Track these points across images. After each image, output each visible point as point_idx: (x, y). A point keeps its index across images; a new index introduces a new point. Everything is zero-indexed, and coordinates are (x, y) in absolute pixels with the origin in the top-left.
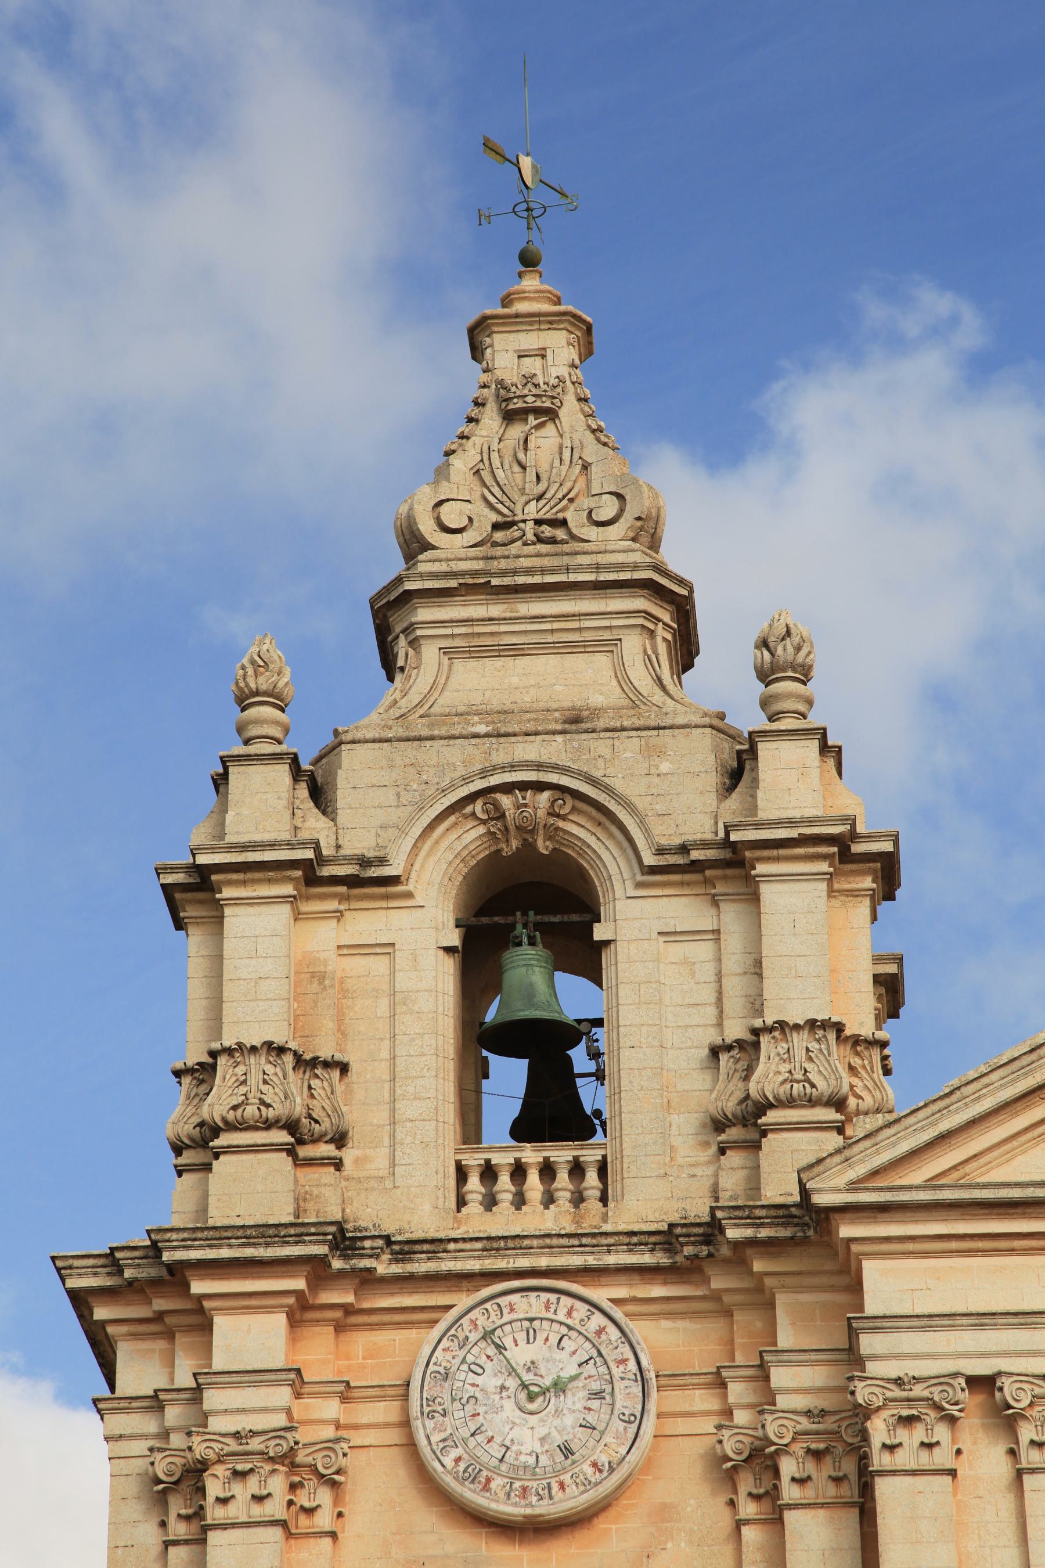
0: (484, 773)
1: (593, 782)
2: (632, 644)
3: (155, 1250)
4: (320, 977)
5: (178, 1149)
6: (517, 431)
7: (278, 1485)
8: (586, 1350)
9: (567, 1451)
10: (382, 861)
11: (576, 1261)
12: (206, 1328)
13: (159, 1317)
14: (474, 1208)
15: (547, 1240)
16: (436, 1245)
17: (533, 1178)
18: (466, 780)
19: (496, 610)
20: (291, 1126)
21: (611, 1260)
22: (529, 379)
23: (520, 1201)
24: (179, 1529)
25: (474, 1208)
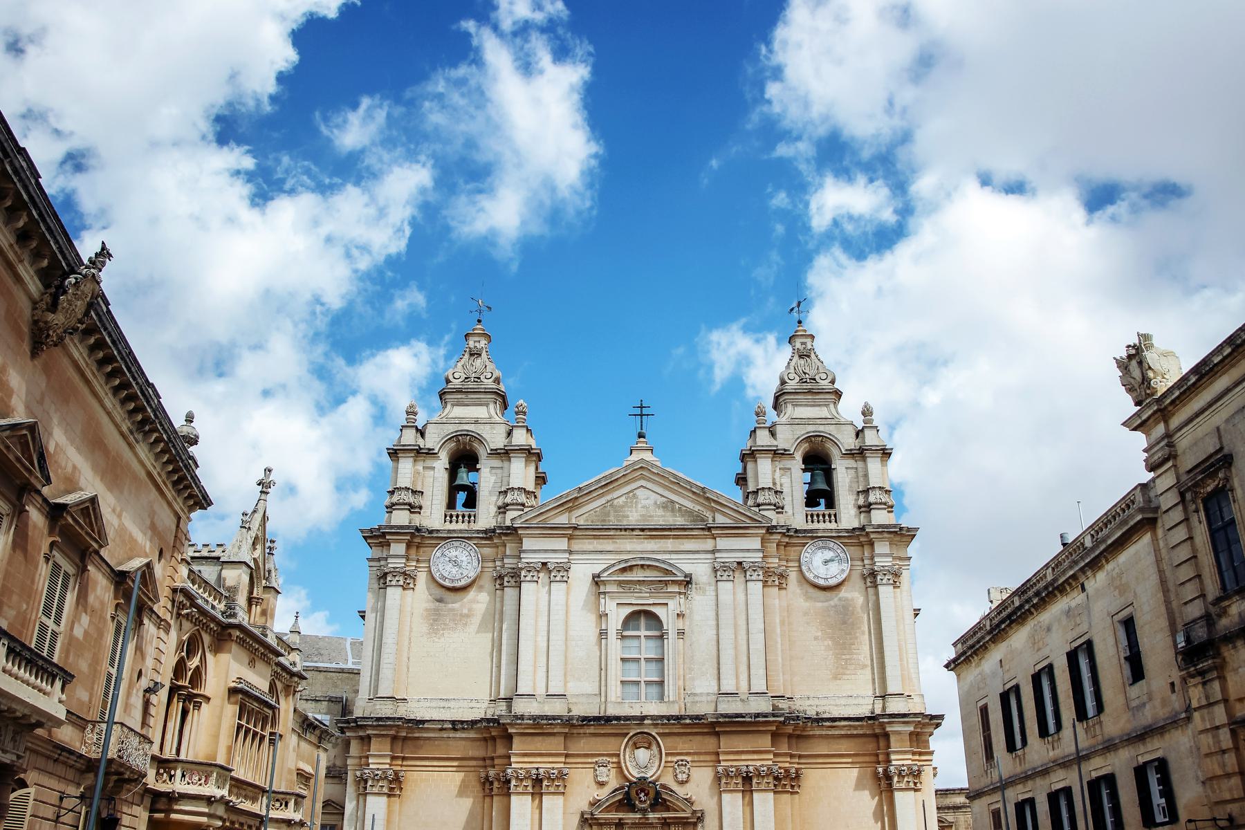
0: (456, 432)
1: (478, 434)
2: (492, 406)
3: (379, 529)
4: (419, 473)
5: (387, 507)
6: (472, 358)
7: (401, 579)
8: (467, 554)
10: (433, 449)
11: (467, 535)
12: (389, 545)
13: (381, 542)
14: (448, 523)
15: (461, 531)
16: (438, 531)
17: (460, 518)
18: (452, 433)
19: (463, 396)
20: (410, 504)
22: (475, 347)
24: (382, 586)
25: (448, 523)
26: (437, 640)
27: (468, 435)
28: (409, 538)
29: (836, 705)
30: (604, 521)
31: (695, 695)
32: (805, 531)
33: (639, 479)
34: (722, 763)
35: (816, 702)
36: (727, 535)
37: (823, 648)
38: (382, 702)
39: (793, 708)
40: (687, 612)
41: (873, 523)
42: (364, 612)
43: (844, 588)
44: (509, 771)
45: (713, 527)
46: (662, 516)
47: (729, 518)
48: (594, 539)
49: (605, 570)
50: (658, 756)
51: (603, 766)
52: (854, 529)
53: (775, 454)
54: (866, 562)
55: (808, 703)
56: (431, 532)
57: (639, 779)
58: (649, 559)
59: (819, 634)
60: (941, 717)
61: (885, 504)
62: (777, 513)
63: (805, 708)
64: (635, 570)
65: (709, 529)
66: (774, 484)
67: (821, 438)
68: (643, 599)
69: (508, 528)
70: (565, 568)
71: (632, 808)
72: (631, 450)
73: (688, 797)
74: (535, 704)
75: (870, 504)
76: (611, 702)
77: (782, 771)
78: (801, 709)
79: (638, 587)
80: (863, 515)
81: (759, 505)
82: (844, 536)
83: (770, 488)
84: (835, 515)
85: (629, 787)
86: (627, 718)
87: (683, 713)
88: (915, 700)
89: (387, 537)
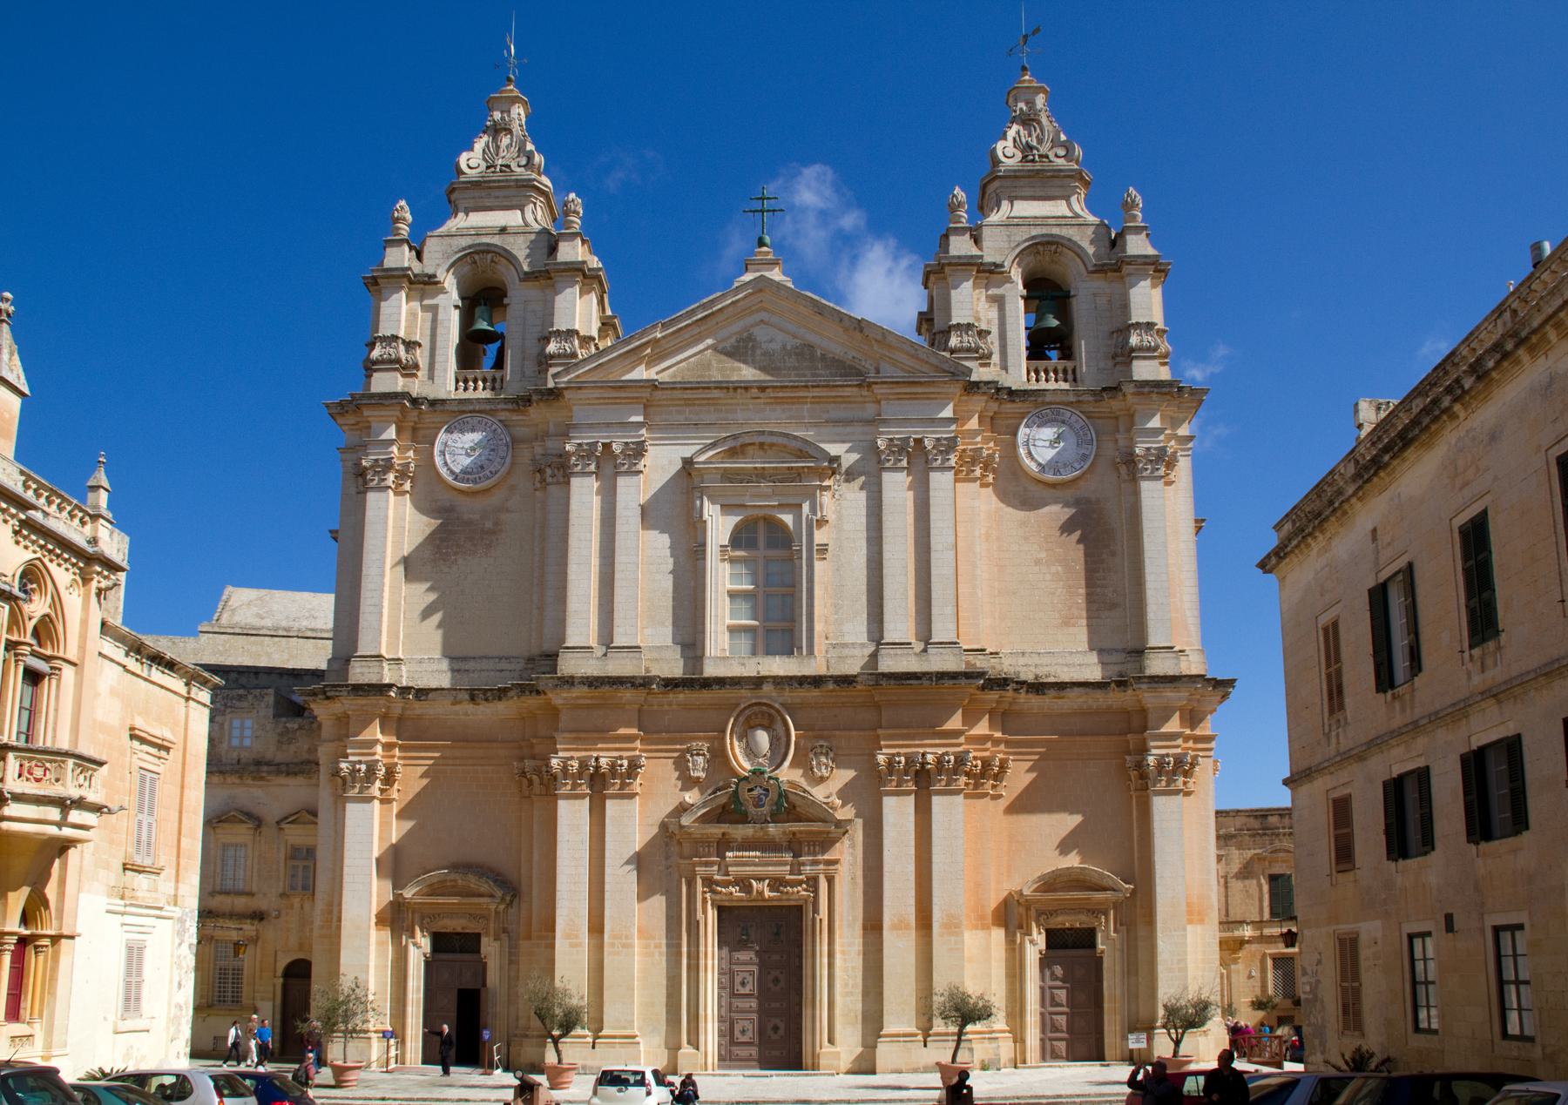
9: (482, 467)
21: (499, 407)
23: (475, 389)
26: (446, 570)
27: (488, 252)
28: (398, 414)
29: (1066, 665)
30: (702, 376)
31: (844, 645)
32: (1025, 392)
33: (758, 311)
34: (884, 751)
35: (1036, 660)
36: (899, 397)
37: (1048, 577)
38: (364, 663)
39: (998, 667)
40: (831, 517)
41: (1135, 378)
42: (337, 532)
43: (1082, 483)
44: (554, 762)
45: (876, 383)
46: (795, 368)
47: (902, 370)
48: (690, 405)
49: (701, 452)
50: (784, 739)
51: (698, 755)
52: (1104, 389)
53: (978, 272)
54: (1122, 443)
55: (1022, 661)
56: (433, 403)
57: (754, 772)
58: (771, 433)
59: (1043, 555)
60: (1230, 683)
61: (1156, 348)
62: (982, 365)
63: (1018, 669)
64: (750, 450)
65: (870, 385)
66: (978, 319)
67: (1054, 247)
68: (762, 499)
69: (551, 392)
70: (639, 451)
71: (744, 819)
72: (747, 265)
73: (829, 800)
74: (594, 662)
75: (1133, 350)
76: (711, 657)
77: (979, 762)
78: (1012, 670)
79: (754, 479)
80: (1118, 368)
81: (952, 351)
82: (1089, 402)
83: (969, 324)
84: (1074, 371)
85: (737, 784)
86: (736, 682)
87: (823, 671)
88: (1191, 658)
89: (366, 413)
